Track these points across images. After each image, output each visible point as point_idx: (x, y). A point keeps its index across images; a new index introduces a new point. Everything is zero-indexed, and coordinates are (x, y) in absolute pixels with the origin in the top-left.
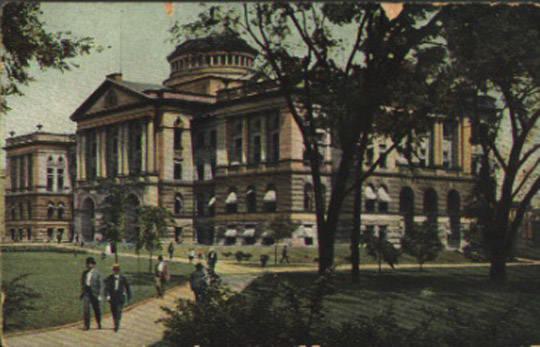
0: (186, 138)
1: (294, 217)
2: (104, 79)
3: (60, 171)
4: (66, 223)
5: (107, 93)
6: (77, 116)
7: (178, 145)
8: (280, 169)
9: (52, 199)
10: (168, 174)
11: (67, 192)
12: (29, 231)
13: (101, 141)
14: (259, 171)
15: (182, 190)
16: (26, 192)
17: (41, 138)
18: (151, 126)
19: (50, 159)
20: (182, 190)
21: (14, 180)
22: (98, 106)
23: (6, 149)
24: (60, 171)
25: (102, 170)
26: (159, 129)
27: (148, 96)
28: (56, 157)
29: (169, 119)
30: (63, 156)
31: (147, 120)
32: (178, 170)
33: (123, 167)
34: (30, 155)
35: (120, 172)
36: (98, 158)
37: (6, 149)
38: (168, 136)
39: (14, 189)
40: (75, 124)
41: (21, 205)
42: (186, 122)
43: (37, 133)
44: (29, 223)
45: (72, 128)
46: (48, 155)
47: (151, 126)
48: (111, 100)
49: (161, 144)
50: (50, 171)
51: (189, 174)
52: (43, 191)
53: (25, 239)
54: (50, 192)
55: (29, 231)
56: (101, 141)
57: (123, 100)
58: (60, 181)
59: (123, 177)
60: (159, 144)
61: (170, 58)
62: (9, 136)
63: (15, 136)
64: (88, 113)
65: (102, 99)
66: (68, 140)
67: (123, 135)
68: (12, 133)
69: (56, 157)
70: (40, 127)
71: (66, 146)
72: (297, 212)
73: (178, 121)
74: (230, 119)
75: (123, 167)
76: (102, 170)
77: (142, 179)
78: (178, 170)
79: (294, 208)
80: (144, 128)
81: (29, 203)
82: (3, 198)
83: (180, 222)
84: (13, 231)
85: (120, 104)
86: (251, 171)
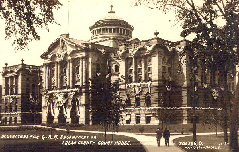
62: (5, 66)
63: (8, 66)
68: (6, 64)
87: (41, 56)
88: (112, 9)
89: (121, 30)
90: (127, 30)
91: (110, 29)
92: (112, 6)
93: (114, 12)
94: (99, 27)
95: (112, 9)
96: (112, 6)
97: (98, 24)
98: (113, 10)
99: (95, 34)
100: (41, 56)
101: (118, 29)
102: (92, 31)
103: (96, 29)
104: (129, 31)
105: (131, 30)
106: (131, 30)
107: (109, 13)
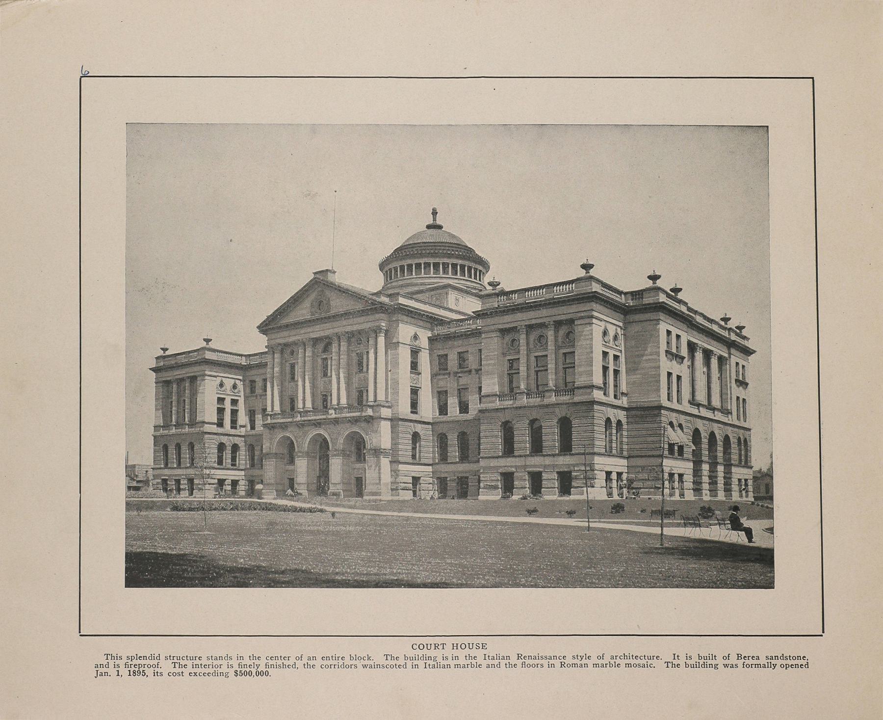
0: (424, 358)
1: (597, 460)
2: (312, 276)
3: (234, 402)
4: (243, 473)
5: (313, 296)
6: (265, 328)
7: (414, 366)
8: (577, 399)
9: (224, 439)
10: (404, 408)
11: (242, 431)
12: (191, 481)
13: (305, 358)
14: (546, 401)
15: (419, 428)
16: (187, 430)
17: (209, 355)
18: (381, 340)
19: (221, 385)
20: (419, 428)
21: (167, 416)
22: (303, 312)
23: (155, 370)
24: (234, 402)
25: (305, 399)
26: (392, 345)
27: (378, 299)
28: (228, 383)
29: (406, 331)
30: (240, 385)
31: (376, 331)
32: (414, 405)
33: (340, 394)
34: (193, 379)
35: (335, 402)
36: (300, 383)
37: (155, 370)
38: (405, 355)
39: (166, 426)
40: (264, 338)
41: (178, 447)
42: (424, 335)
43: (203, 349)
44: (191, 472)
45: (258, 343)
46: (219, 380)
47: (381, 340)
48: (320, 304)
49: (396, 364)
50: (221, 400)
51: (428, 408)
52: (214, 428)
53: (184, 494)
54: (220, 430)
55: (191, 481)
56: (305, 358)
57: (338, 304)
58: (234, 413)
59: (339, 409)
60: (392, 365)
61: (315, 273)
62: (161, 353)
63: (167, 353)
64: (285, 321)
65: (307, 304)
66: (243, 362)
67: (340, 355)
68: (165, 350)
69: (228, 383)
70: (208, 341)
71: (249, 370)
72: (599, 454)
73: (416, 337)
74: (504, 332)
75: (340, 394)
76: (305, 399)
77: (370, 412)
78: (414, 405)
79: (596, 450)
80: (371, 342)
81: (191, 446)
82: (152, 441)
83: (416, 470)
84: (165, 481)
85: (333, 312)
86: (535, 401)
87: (258, 327)
88: (434, 219)
89: (470, 268)
90: (476, 269)
91: (436, 265)
92: (434, 213)
93: (440, 227)
94: (405, 260)
95: (434, 219)
96: (434, 213)
97: (401, 252)
98: (438, 222)
99: (391, 279)
100: (258, 327)
101: (454, 266)
102: (387, 268)
103: (397, 264)
104: (480, 271)
105: (484, 270)
106: (484, 270)
107: (429, 227)
